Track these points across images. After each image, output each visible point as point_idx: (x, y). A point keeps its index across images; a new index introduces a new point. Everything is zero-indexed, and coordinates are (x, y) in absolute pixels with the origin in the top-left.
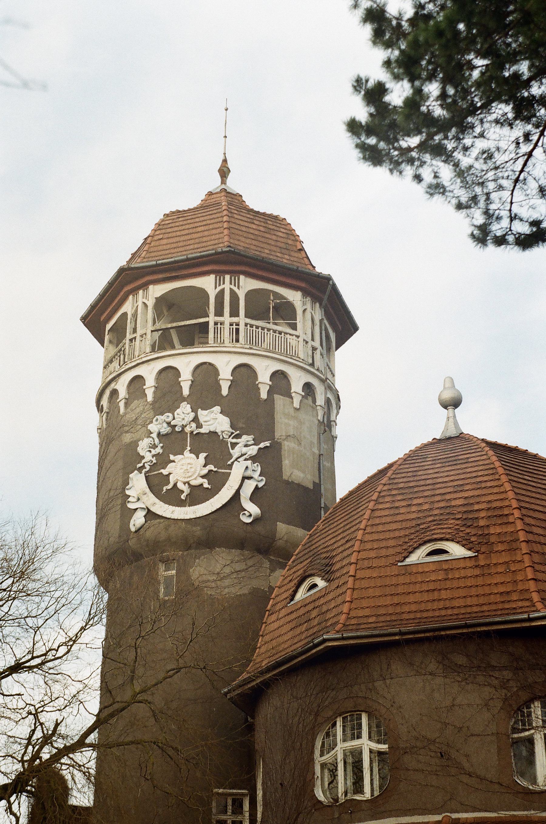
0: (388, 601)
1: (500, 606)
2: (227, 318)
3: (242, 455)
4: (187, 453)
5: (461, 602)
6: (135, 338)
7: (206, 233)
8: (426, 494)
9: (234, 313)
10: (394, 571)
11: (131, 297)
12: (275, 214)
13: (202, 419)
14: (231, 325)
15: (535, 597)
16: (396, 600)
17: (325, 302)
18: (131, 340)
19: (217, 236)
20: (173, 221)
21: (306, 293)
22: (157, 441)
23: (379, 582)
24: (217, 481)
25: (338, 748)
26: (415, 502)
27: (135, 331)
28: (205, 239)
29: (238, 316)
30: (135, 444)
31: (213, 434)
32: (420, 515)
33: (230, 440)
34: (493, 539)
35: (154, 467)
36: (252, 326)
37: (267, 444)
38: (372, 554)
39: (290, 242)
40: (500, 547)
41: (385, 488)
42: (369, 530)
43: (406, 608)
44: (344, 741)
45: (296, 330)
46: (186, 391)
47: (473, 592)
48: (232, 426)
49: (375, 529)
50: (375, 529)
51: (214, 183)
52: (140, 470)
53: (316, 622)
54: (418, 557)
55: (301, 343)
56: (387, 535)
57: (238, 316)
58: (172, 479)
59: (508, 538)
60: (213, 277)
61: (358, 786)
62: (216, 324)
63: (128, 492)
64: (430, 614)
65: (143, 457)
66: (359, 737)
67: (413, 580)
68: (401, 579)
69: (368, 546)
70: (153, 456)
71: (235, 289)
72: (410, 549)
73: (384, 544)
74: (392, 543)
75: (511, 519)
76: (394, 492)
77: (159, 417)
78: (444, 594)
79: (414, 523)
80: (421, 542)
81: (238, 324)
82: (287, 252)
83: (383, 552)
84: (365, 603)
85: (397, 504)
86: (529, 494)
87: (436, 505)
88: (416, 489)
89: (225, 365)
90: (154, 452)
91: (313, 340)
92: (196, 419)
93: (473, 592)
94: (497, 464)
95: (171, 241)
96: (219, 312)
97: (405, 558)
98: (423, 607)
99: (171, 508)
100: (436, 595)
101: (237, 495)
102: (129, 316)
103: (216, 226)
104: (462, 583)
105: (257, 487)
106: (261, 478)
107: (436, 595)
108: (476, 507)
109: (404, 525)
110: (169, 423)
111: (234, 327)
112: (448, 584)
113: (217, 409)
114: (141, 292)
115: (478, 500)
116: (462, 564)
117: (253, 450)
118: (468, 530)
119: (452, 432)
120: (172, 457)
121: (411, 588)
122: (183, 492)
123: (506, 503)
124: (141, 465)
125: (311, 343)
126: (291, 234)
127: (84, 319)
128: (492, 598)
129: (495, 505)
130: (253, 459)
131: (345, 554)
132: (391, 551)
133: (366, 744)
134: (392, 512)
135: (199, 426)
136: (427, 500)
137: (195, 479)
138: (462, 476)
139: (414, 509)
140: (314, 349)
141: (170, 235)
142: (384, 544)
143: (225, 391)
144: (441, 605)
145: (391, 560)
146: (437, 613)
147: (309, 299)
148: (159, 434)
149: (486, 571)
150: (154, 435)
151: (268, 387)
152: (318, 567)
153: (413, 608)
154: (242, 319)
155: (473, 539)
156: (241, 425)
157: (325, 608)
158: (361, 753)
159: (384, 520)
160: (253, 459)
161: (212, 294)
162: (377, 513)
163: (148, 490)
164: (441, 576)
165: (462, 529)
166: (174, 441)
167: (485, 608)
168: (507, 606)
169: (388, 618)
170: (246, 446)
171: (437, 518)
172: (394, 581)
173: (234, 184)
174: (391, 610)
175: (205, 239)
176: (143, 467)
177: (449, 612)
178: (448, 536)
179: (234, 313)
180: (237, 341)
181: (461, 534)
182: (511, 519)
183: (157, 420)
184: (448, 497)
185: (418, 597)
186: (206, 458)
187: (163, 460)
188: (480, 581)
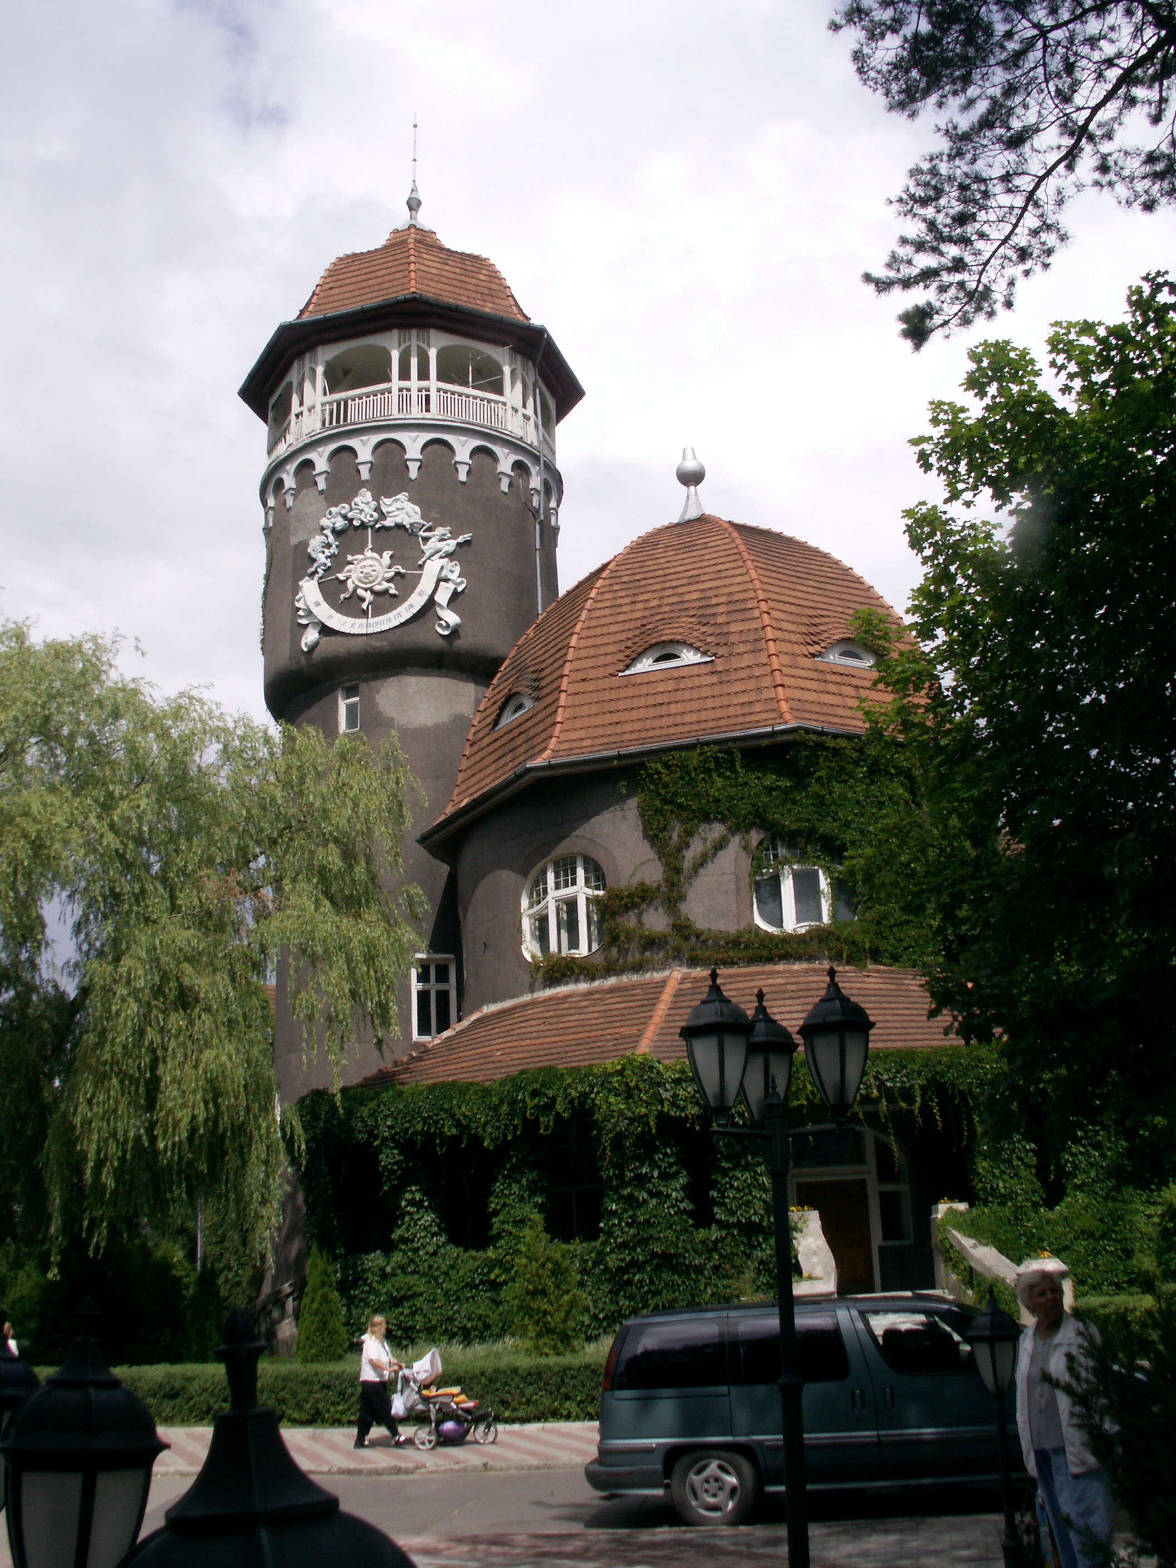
0: (608, 719)
1: (741, 720)
2: (414, 383)
3: (437, 552)
4: (369, 553)
5: (695, 717)
6: (301, 413)
7: (387, 278)
8: (654, 587)
9: (424, 375)
10: (615, 682)
11: (296, 363)
12: (476, 253)
13: (384, 510)
14: (420, 390)
15: (784, 706)
16: (616, 717)
17: (538, 361)
18: (297, 416)
19: (401, 281)
20: (348, 268)
21: (516, 350)
22: (331, 539)
23: (595, 697)
24: (406, 583)
25: (549, 897)
26: (641, 598)
27: (301, 404)
28: (386, 285)
30: (305, 544)
31: (400, 526)
32: (646, 613)
33: (421, 533)
34: (733, 638)
35: (328, 570)
36: (446, 392)
37: (467, 537)
38: (588, 663)
39: (494, 286)
40: (742, 648)
41: (608, 582)
42: (584, 634)
43: (628, 727)
44: (557, 887)
45: (501, 394)
46: (365, 474)
47: (709, 703)
48: (423, 517)
49: (592, 632)
50: (592, 632)
51: (402, 219)
52: (312, 575)
53: (522, 749)
54: (645, 665)
55: (510, 411)
56: (606, 639)
58: (350, 585)
59: (752, 637)
60: (395, 332)
61: (574, 943)
62: (401, 390)
63: (297, 605)
64: (657, 733)
65: (314, 560)
66: (574, 882)
67: (637, 693)
68: (624, 693)
69: (584, 653)
70: (327, 557)
71: (425, 346)
72: (634, 655)
73: (602, 650)
74: (611, 649)
75: (756, 613)
76: (616, 587)
77: (334, 510)
78: (673, 709)
79: (639, 623)
80: (646, 645)
81: (428, 390)
82: (490, 299)
83: (602, 660)
84: (578, 723)
85: (619, 602)
86: (779, 583)
87: (667, 601)
88: (643, 583)
89: (413, 444)
90: (327, 552)
91: (524, 407)
92: (378, 509)
93: (709, 703)
94: (742, 548)
95: (344, 289)
96: (405, 375)
97: (628, 667)
98: (648, 724)
99: (351, 620)
100: (664, 710)
101: (431, 603)
102: (295, 385)
103: (398, 268)
104: (695, 694)
105: (455, 591)
106: (459, 580)
107: (664, 710)
108: (714, 601)
109: (627, 626)
110: (345, 517)
111: (424, 393)
112: (679, 696)
113: (403, 496)
114: (308, 356)
115: (716, 592)
116: (696, 670)
117: (451, 545)
118: (704, 629)
119: (692, 514)
120: (350, 558)
121: (635, 703)
122: (363, 600)
123: (752, 594)
124: (313, 569)
125: (521, 410)
126: (494, 276)
128: (732, 711)
129: (736, 597)
130: (450, 556)
131: (556, 665)
132: (610, 659)
133: (581, 891)
134: (614, 610)
135: (383, 516)
136: (656, 595)
137: (380, 584)
138: (698, 565)
139: (639, 606)
140: (526, 418)
141: (343, 283)
142: (602, 650)
143: (413, 473)
144: (671, 721)
145: (610, 670)
146: (665, 732)
147: (519, 357)
148: (333, 531)
149: (725, 677)
150: (328, 532)
151: (467, 468)
152: (525, 683)
153: (638, 726)
154: (433, 383)
155: (709, 639)
156: (434, 515)
157: (532, 733)
158: (576, 903)
159: (603, 621)
160: (450, 556)
161: (395, 355)
162: (595, 614)
163: (321, 599)
164: (671, 685)
165: (697, 627)
166: (350, 536)
167: (722, 723)
168: (748, 719)
169: (607, 740)
170: (442, 540)
171: (666, 616)
172: (614, 695)
173: (425, 219)
174: (609, 730)
175: (386, 285)
176: (316, 572)
177: (680, 729)
178: (679, 637)
179: (424, 375)
180: (428, 410)
181: (695, 634)
182: (756, 613)
183: (330, 513)
184: (681, 590)
185: (643, 713)
186: (391, 557)
187: (339, 562)
188: (717, 690)
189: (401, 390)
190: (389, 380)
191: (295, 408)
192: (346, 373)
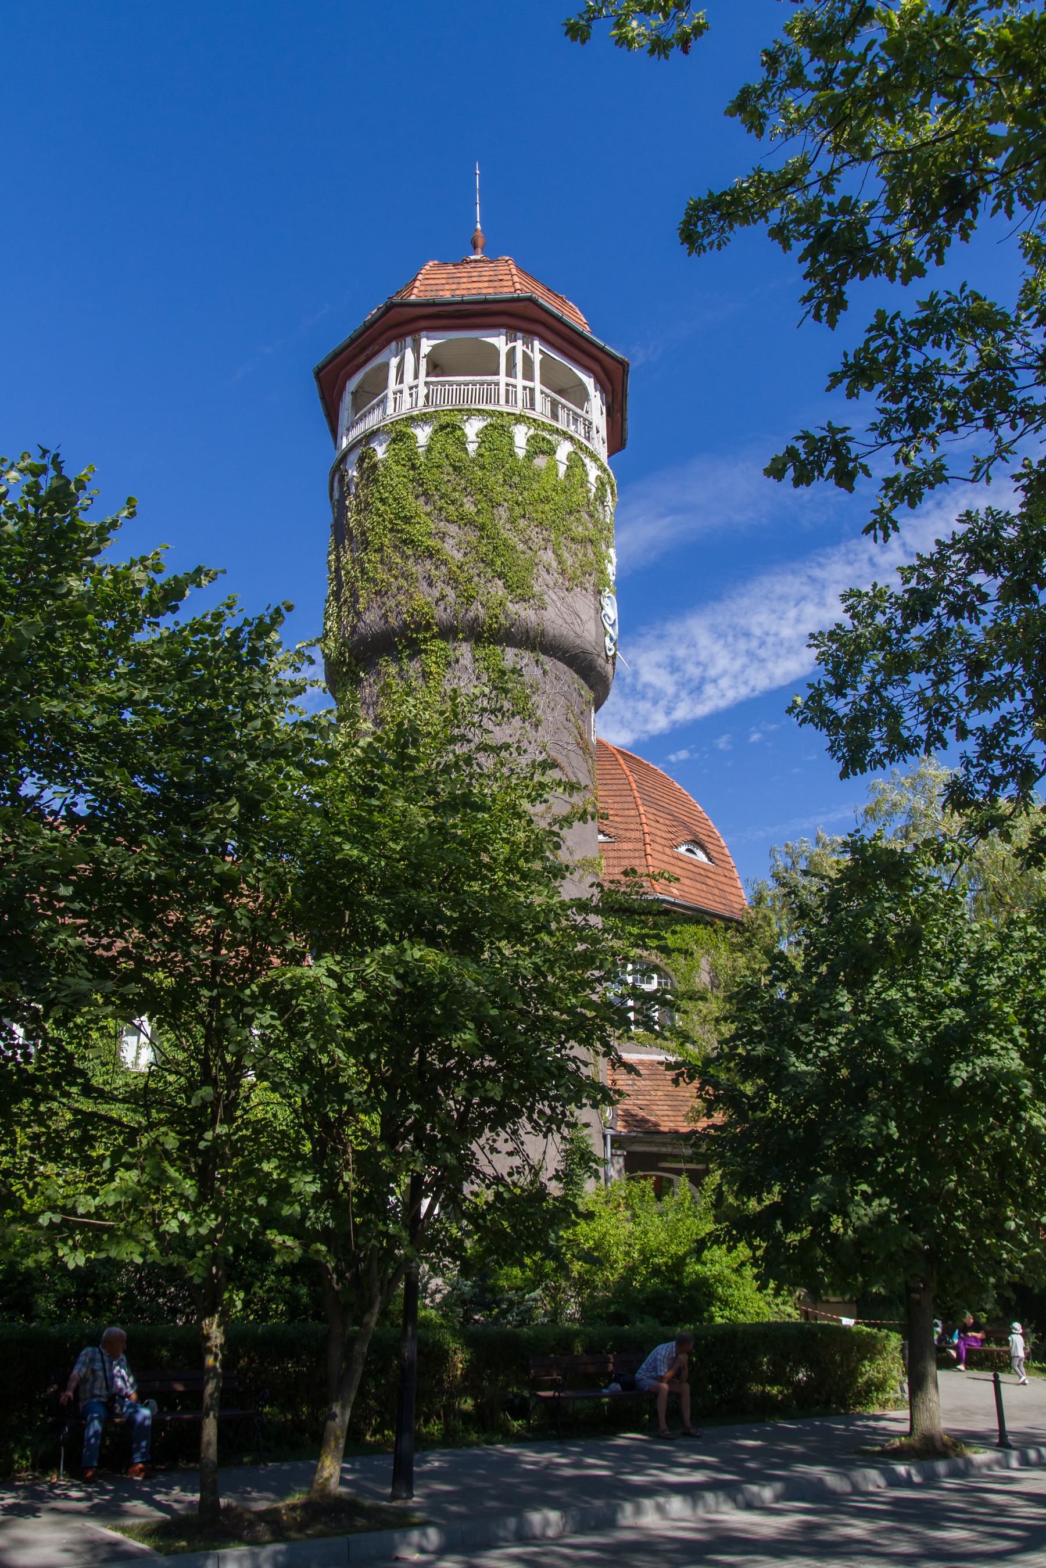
11: (394, 344)
18: (395, 393)
29: (532, 379)
57: (532, 379)
62: (507, 385)
71: (529, 352)
81: (532, 390)
96: (511, 372)
127: (318, 373)
154: (537, 385)
179: (528, 375)
189: (507, 385)
190: (497, 373)
191: (392, 385)
192: (438, 370)
